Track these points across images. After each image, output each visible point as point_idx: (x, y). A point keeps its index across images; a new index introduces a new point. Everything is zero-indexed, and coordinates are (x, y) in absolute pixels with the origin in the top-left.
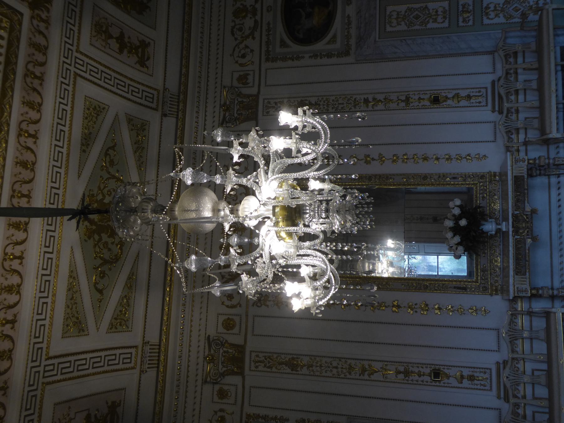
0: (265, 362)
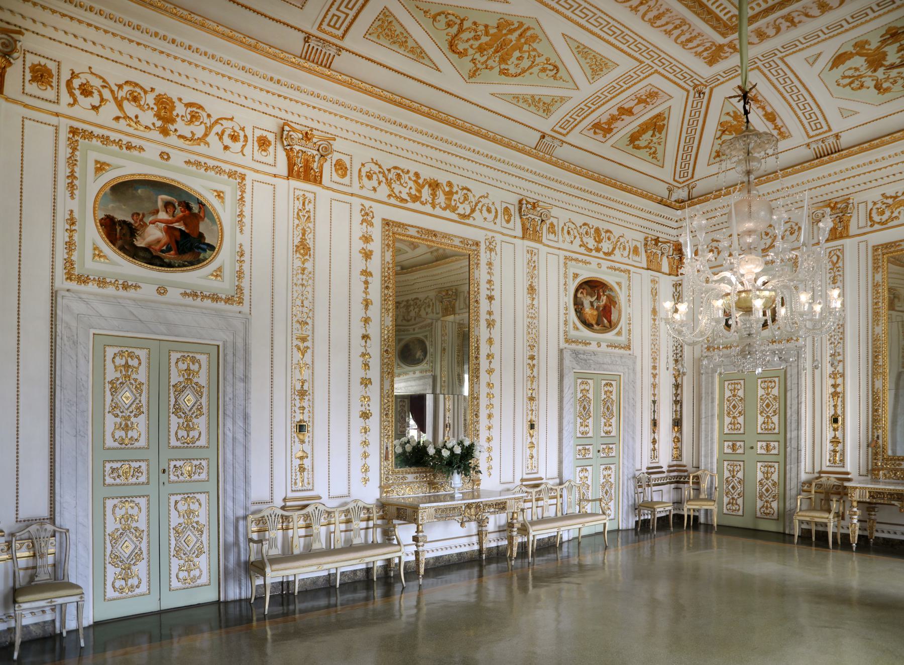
0: (304, 209)
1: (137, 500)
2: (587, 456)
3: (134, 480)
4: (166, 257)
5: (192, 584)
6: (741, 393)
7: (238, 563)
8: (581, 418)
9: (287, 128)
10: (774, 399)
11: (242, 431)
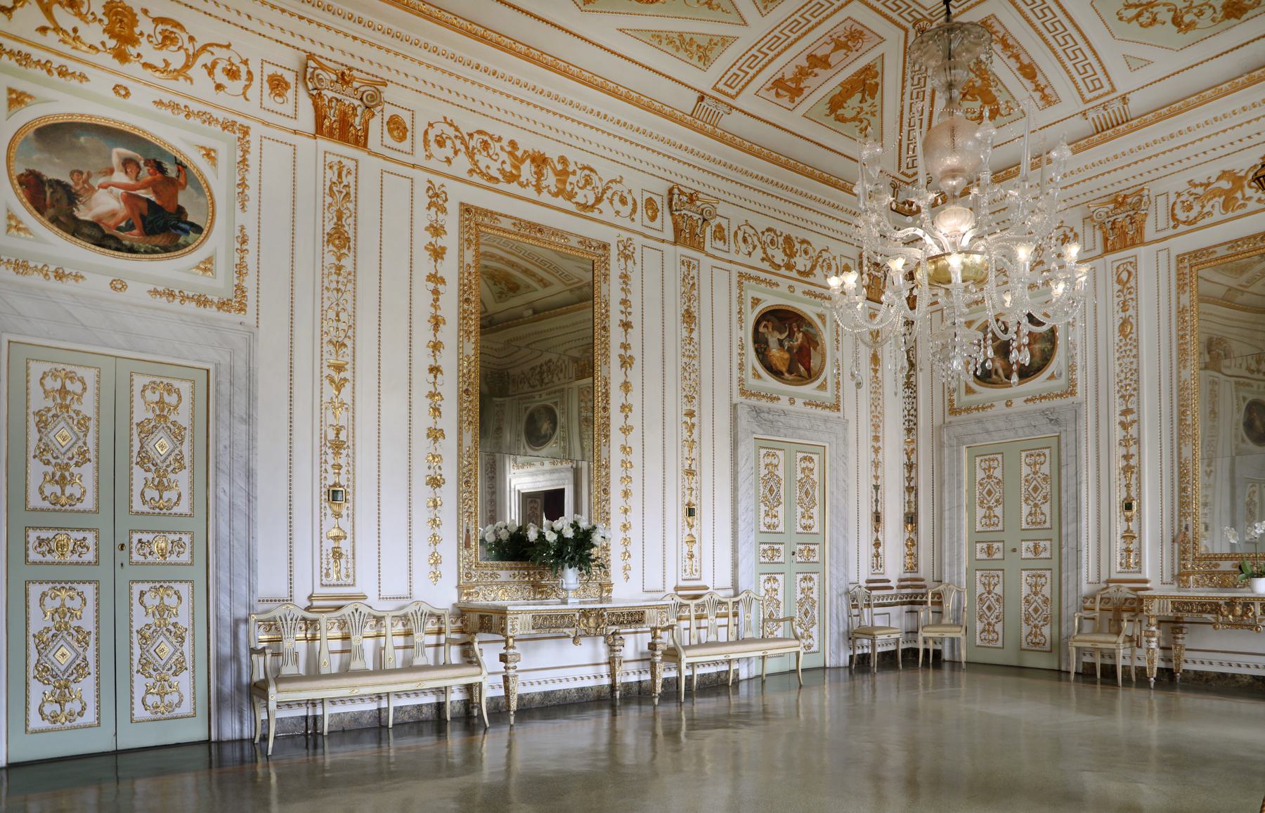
0: (340, 183)
1: (80, 587)
2: (776, 560)
3: (75, 558)
5: (167, 715)
6: (998, 473)
7: (238, 686)
8: (766, 505)
9: (312, 63)
10: (1044, 479)
11: (244, 494)
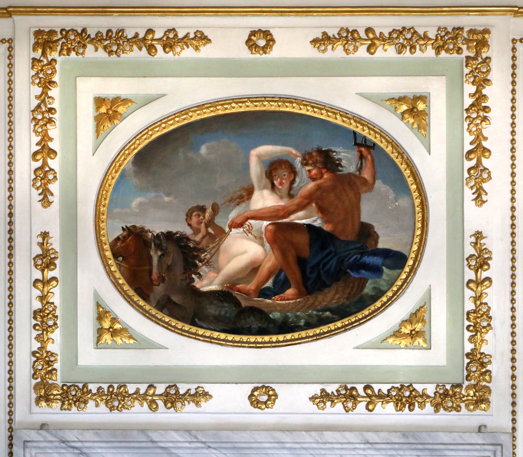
4: (274, 307)
